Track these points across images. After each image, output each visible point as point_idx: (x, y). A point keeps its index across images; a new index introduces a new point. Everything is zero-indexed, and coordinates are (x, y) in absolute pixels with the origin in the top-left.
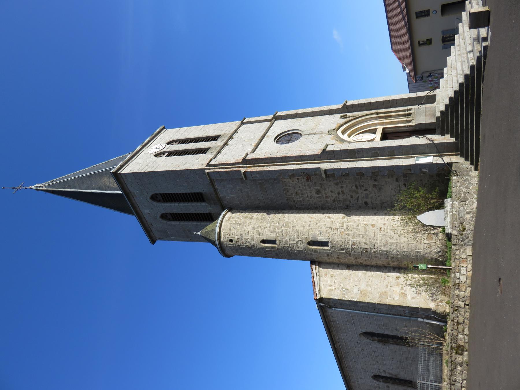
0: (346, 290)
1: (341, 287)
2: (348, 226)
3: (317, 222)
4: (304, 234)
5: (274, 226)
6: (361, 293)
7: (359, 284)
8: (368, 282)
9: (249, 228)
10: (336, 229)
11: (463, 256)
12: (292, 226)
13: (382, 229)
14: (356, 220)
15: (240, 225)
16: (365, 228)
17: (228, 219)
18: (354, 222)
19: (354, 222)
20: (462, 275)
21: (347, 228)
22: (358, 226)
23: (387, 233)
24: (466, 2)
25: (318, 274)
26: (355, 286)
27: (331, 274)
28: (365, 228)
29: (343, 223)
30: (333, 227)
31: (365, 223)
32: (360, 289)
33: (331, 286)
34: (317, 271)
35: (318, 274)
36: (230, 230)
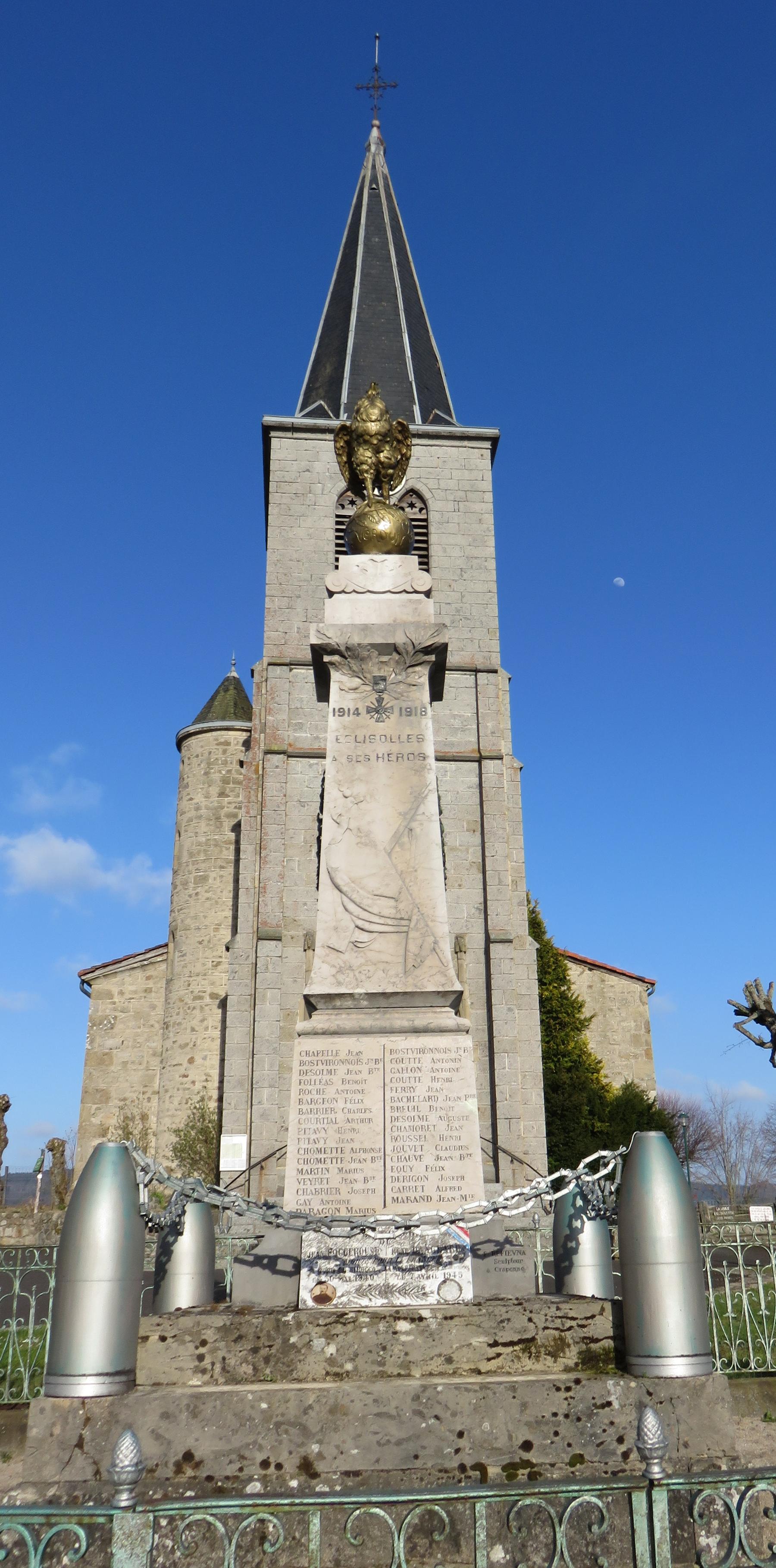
0: (112, 1024)
1: (118, 1014)
2: (194, 1008)
3: (205, 943)
4: (182, 921)
5: (199, 852)
6: (106, 1054)
7: (128, 1048)
8: (133, 1062)
9: (199, 798)
10: (189, 985)
11: (25, 1231)
12: (199, 890)
13: (185, 1079)
14: (205, 1022)
15: (206, 774)
16: (187, 1044)
17: (222, 740)
18: (202, 1021)
19: (202, 1021)
20: (4, 1230)
21: (189, 1008)
22: (193, 1030)
23: (178, 1090)
24: (769, 1210)
25: (146, 963)
26: (122, 1039)
27: (151, 988)
28: (187, 1044)
29: (201, 998)
30: (191, 979)
31: (198, 1043)
32: (115, 1051)
33: (121, 993)
34: (153, 960)
35: (146, 963)
36: (197, 756)
